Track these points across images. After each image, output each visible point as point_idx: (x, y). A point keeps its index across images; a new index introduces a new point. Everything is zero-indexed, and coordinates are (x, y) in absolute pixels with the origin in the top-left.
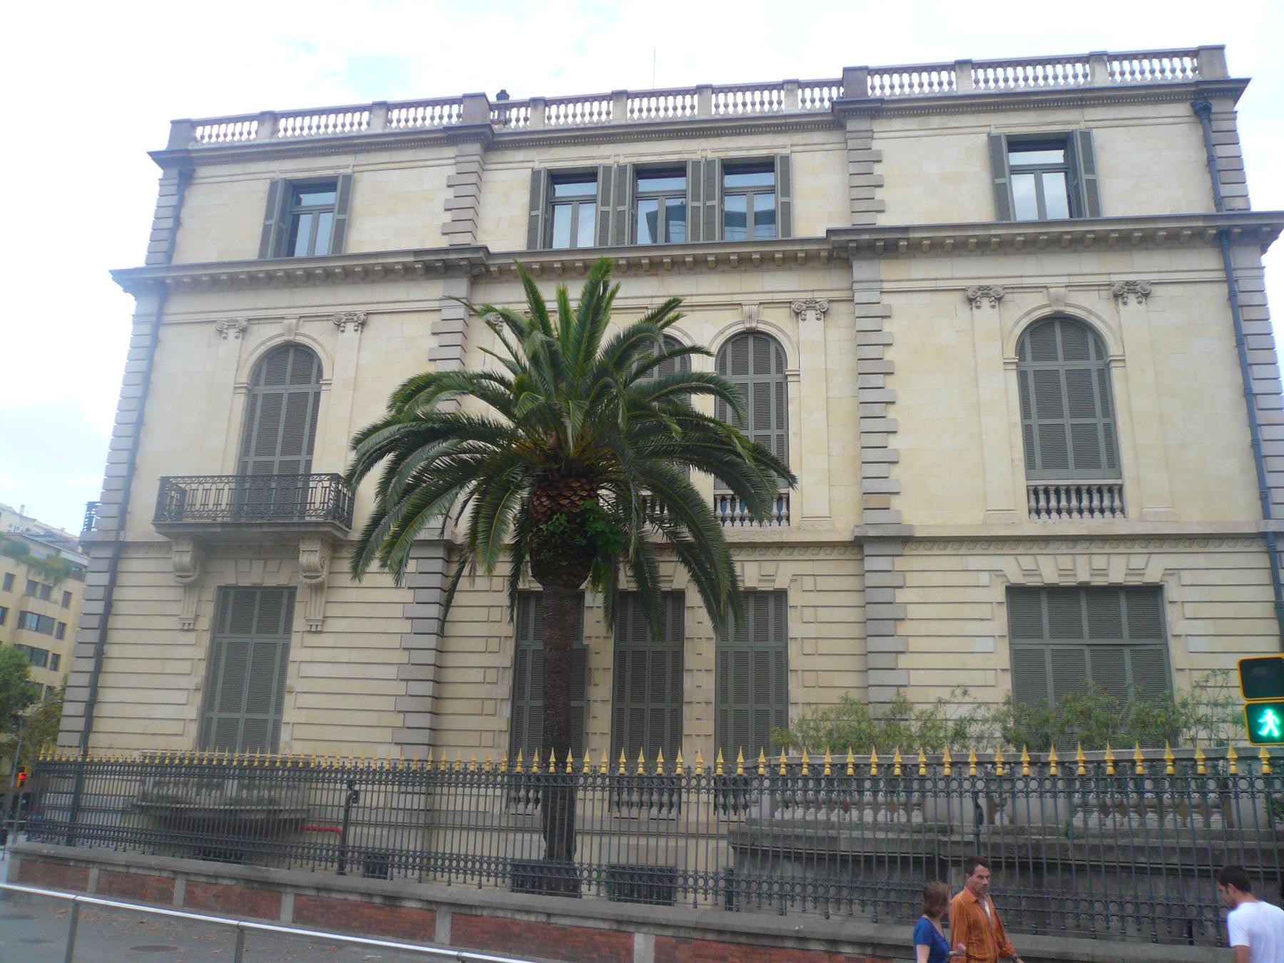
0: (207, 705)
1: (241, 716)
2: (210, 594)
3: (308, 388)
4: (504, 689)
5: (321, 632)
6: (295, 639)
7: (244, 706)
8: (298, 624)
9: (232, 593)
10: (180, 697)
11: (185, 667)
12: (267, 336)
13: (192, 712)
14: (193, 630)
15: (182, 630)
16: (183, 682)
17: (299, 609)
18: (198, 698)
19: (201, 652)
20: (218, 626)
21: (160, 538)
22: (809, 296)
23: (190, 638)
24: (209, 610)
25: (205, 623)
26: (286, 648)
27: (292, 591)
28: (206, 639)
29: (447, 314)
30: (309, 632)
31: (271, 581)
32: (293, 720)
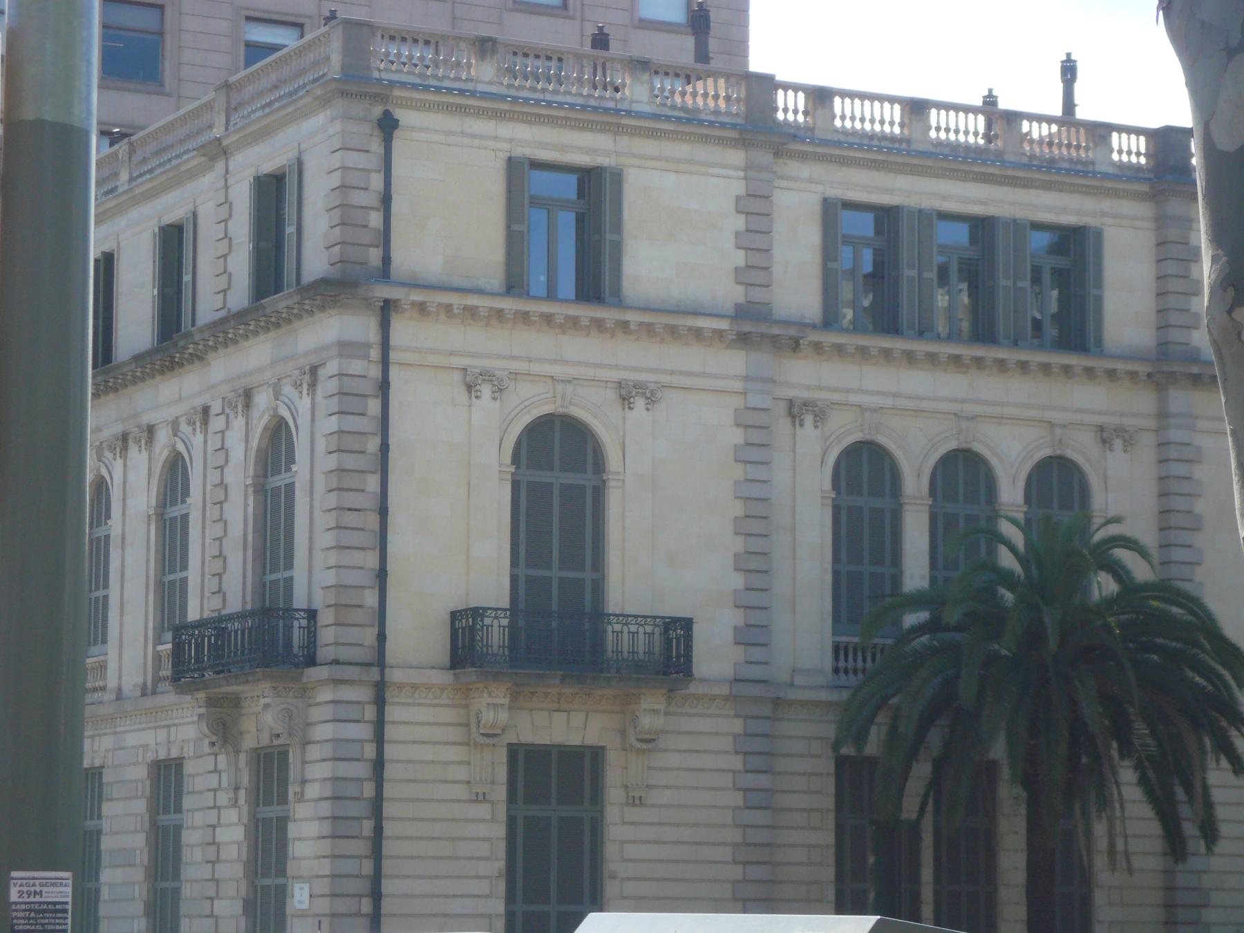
0: (510, 898)
2: (502, 756)
3: (586, 479)
4: (829, 873)
6: (612, 814)
8: (613, 794)
10: (483, 887)
11: (484, 849)
12: (532, 402)
13: (498, 906)
15: (471, 801)
16: (484, 868)
18: (501, 887)
19: (500, 831)
20: (512, 798)
22: (1115, 421)
23: (483, 810)
25: (501, 793)
26: (597, 826)
28: (502, 814)
29: (756, 401)
30: (628, 804)
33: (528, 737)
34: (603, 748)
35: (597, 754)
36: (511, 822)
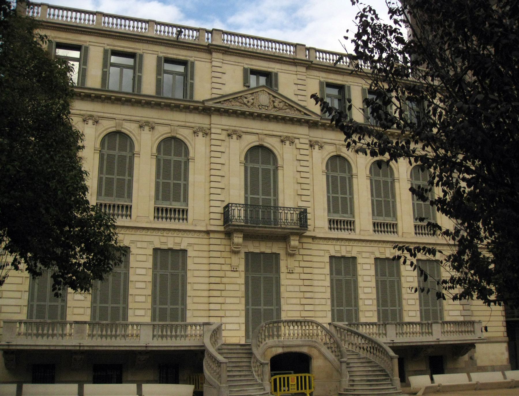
1: (262, 307)
2: (243, 255)
5: (293, 273)
6: (282, 276)
7: (262, 304)
8: (283, 269)
9: (250, 255)
14: (237, 271)
15: (232, 271)
17: (283, 264)
19: (242, 281)
20: (247, 270)
21: (222, 229)
23: (236, 274)
24: (243, 262)
25: (242, 268)
27: (277, 255)
28: (243, 274)
31: (268, 251)
32: (286, 309)
33: (252, 250)
34: (279, 254)
35: (277, 255)
36: (247, 278)
